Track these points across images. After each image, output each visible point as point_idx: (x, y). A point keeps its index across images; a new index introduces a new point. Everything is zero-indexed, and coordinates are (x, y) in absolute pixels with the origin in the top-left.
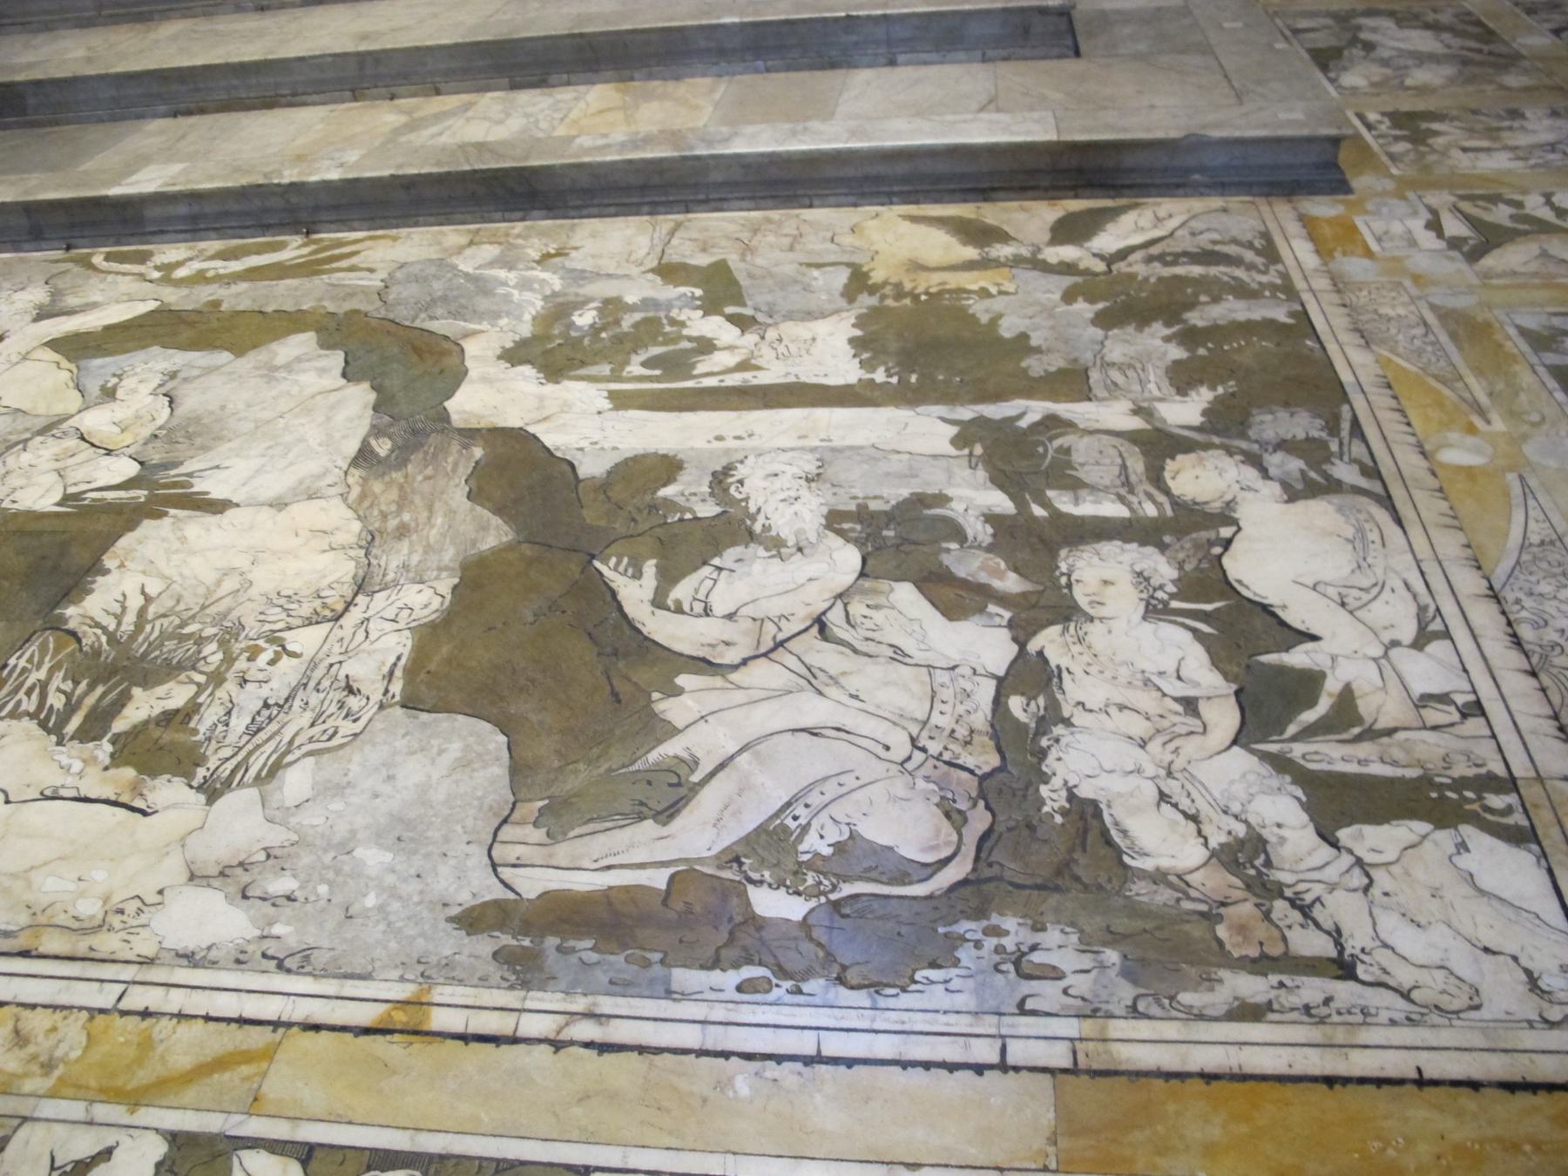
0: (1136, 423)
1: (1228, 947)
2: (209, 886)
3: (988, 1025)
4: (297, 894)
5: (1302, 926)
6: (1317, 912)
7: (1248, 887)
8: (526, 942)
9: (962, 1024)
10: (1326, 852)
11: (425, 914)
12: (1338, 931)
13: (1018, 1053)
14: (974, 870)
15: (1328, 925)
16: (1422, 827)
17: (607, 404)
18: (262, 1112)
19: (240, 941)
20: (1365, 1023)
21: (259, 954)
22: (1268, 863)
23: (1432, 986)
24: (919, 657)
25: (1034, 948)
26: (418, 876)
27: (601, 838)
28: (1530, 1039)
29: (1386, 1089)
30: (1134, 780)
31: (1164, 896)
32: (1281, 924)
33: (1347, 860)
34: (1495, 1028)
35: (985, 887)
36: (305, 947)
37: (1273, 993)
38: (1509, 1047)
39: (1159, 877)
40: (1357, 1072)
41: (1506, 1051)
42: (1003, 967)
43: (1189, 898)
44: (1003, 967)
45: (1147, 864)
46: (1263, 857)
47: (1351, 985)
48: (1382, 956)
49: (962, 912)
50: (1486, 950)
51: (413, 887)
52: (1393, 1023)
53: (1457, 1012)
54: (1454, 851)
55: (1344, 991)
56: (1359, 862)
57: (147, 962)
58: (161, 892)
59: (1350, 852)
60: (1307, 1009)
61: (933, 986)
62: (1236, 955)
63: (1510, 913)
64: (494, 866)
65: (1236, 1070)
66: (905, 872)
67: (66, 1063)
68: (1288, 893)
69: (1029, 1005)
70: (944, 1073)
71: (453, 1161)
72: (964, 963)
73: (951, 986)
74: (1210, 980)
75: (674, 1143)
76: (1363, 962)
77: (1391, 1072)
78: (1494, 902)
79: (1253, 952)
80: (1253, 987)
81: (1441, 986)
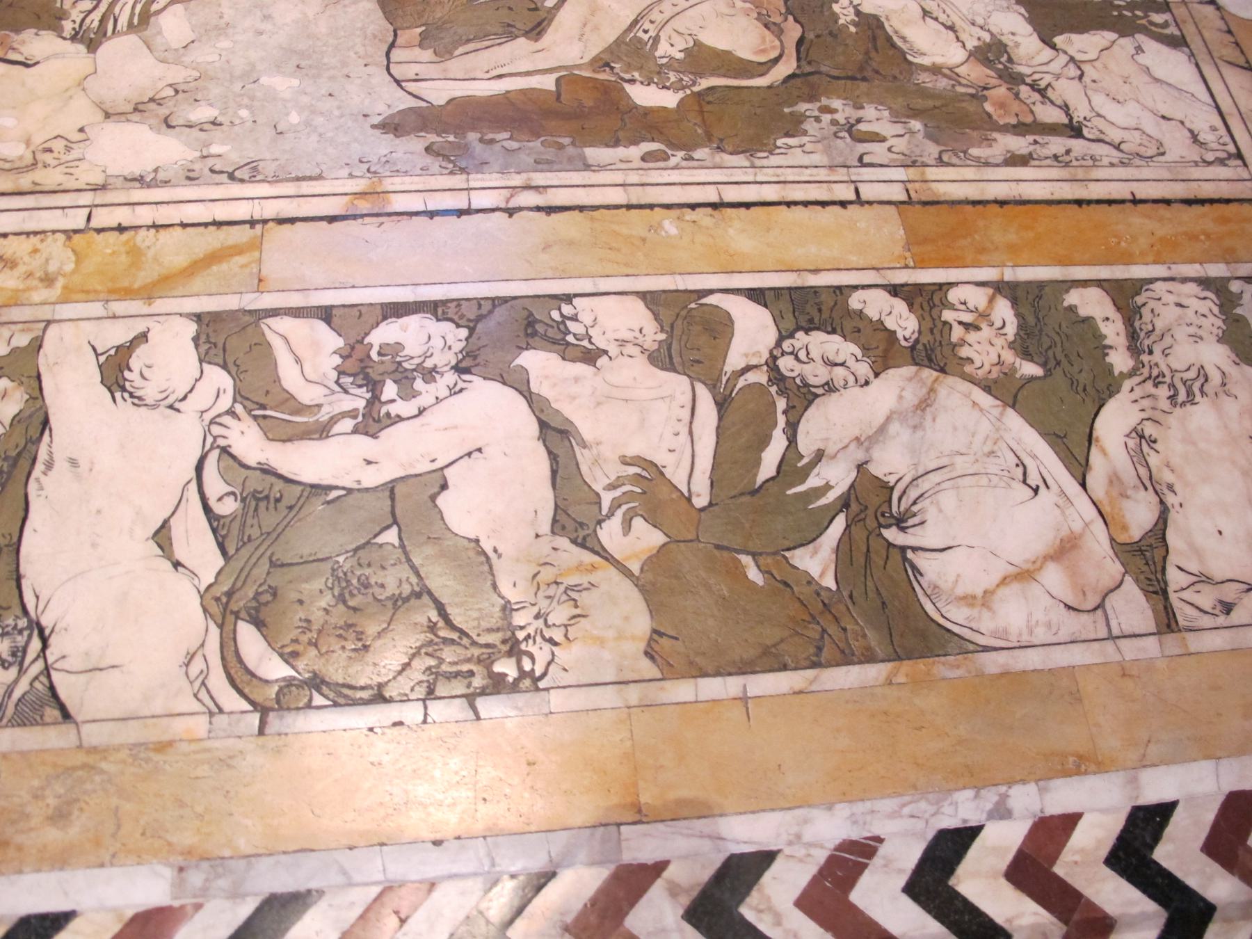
1: (995, 117)
2: (128, 121)
3: (841, 174)
4: (220, 119)
5: (1042, 103)
7: (1000, 77)
8: (451, 138)
9: (822, 174)
10: (1047, 53)
11: (350, 124)
12: (1066, 106)
14: (798, 67)
15: (1059, 102)
16: (1112, 36)
18: (271, 289)
19: (184, 162)
20: (1094, 166)
21: (207, 171)
22: (1010, 60)
23: (1133, 142)
25: (859, 121)
26: (330, 95)
27: (486, 53)
28: (1197, 173)
29: (1114, 206)
31: (943, 83)
32: (1028, 102)
33: (1063, 59)
34: (1175, 167)
35: (810, 78)
36: (250, 160)
37: (1032, 148)
38: (1184, 178)
39: (936, 70)
40: (1095, 196)
41: (1183, 180)
42: (841, 134)
43: (960, 84)
44: (841, 134)
45: (926, 61)
46: (1006, 56)
47: (1080, 142)
48: (1097, 122)
49: (798, 97)
50: (1163, 117)
51: (329, 104)
52: (1112, 165)
53: (1151, 157)
54: (1134, 52)
55: (1077, 145)
56: (1072, 59)
58: (81, 130)
59: (1065, 53)
60: (1056, 157)
61: (793, 150)
62: (1001, 123)
63: (1176, 93)
64: (398, 82)
65: (1018, 198)
67: (64, 275)
68: (1028, 80)
69: (866, 159)
70: (819, 208)
71: (455, 303)
72: (811, 132)
73: (806, 148)
74: (988, 140)
75: (630, 271)
76: (1086, 126)
77: (1115, 196)
78: (1164, 86)
79: (1013, 121)
80: (1020, 144)
81: (1139, 141)
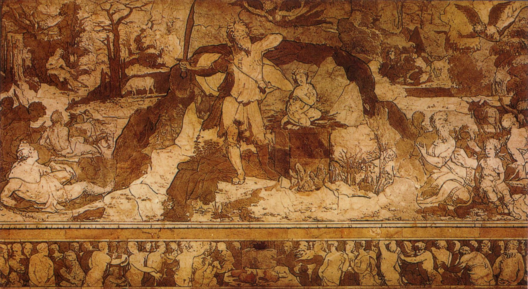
0: (499, 104)
3: (473, 222)
6: (508, 207)
13: (477, 225)
17: (405, 94)
24: (465, 165)
25: (478, 212)
30: (491, 187)
45: (491, 201)
57: (382, 220)
66: (465, 202)
